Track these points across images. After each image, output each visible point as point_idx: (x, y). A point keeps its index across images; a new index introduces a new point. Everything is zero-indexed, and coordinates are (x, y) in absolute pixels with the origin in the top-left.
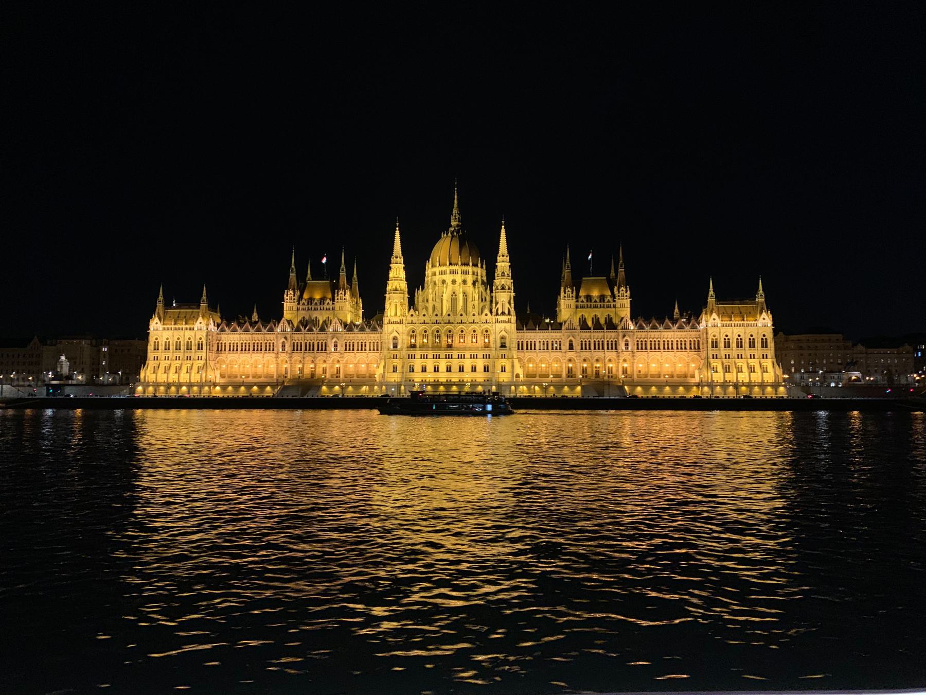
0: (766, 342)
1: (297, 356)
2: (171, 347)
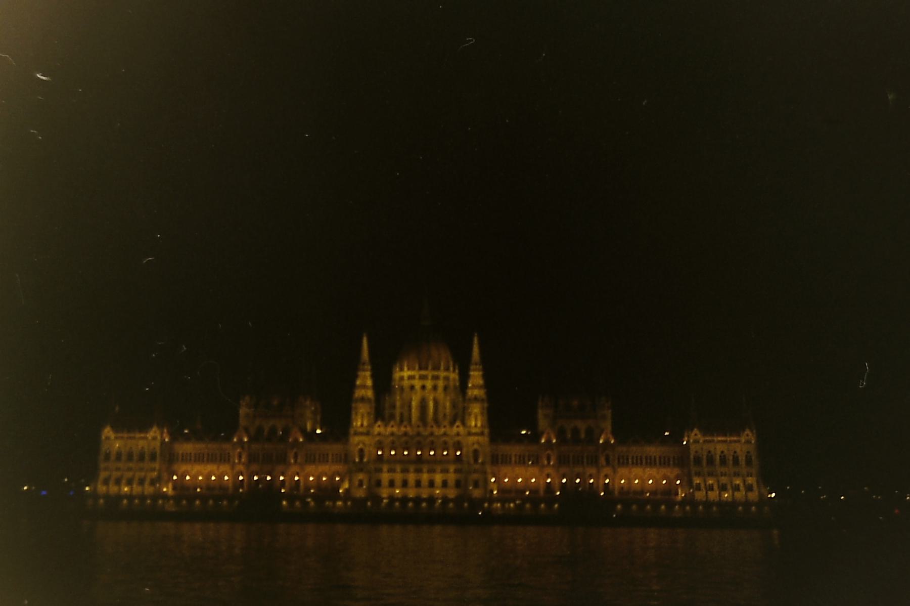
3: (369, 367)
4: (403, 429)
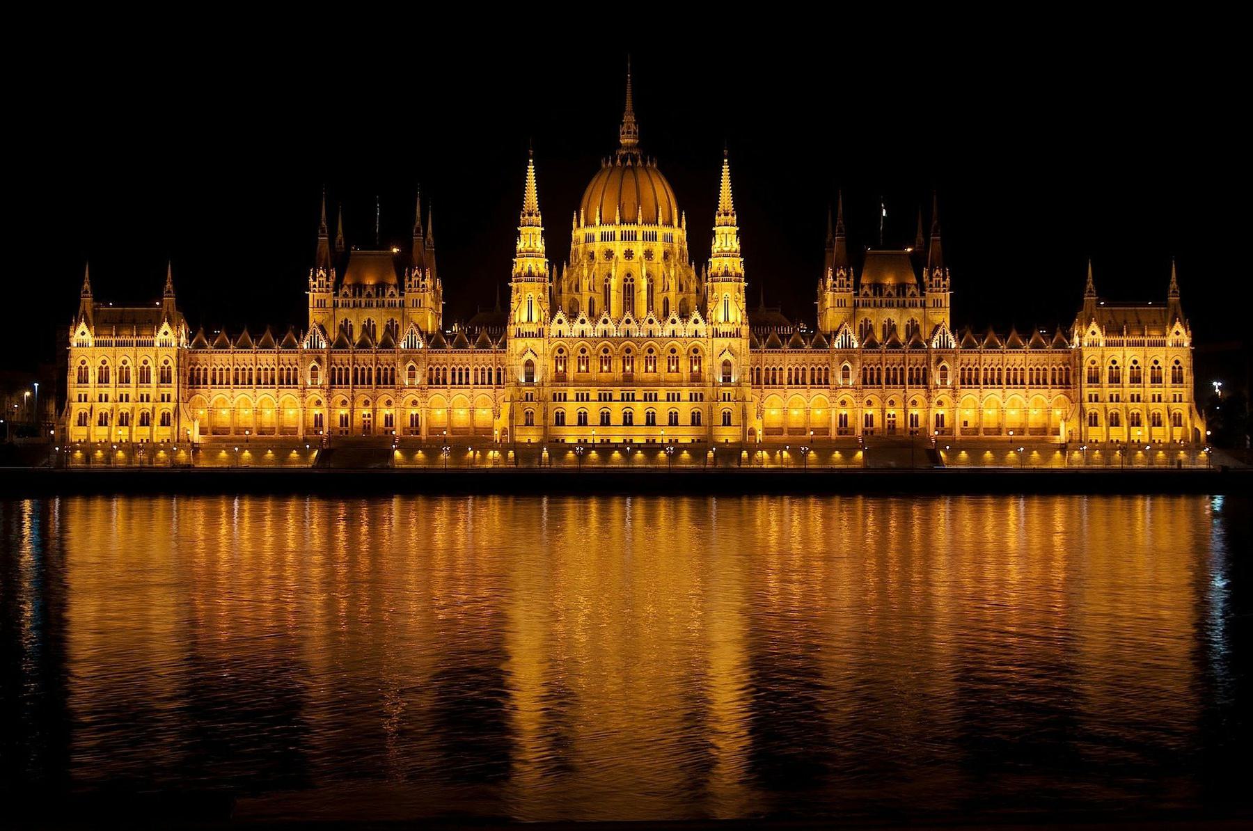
0: (1181, 373)
1: (340, 394)
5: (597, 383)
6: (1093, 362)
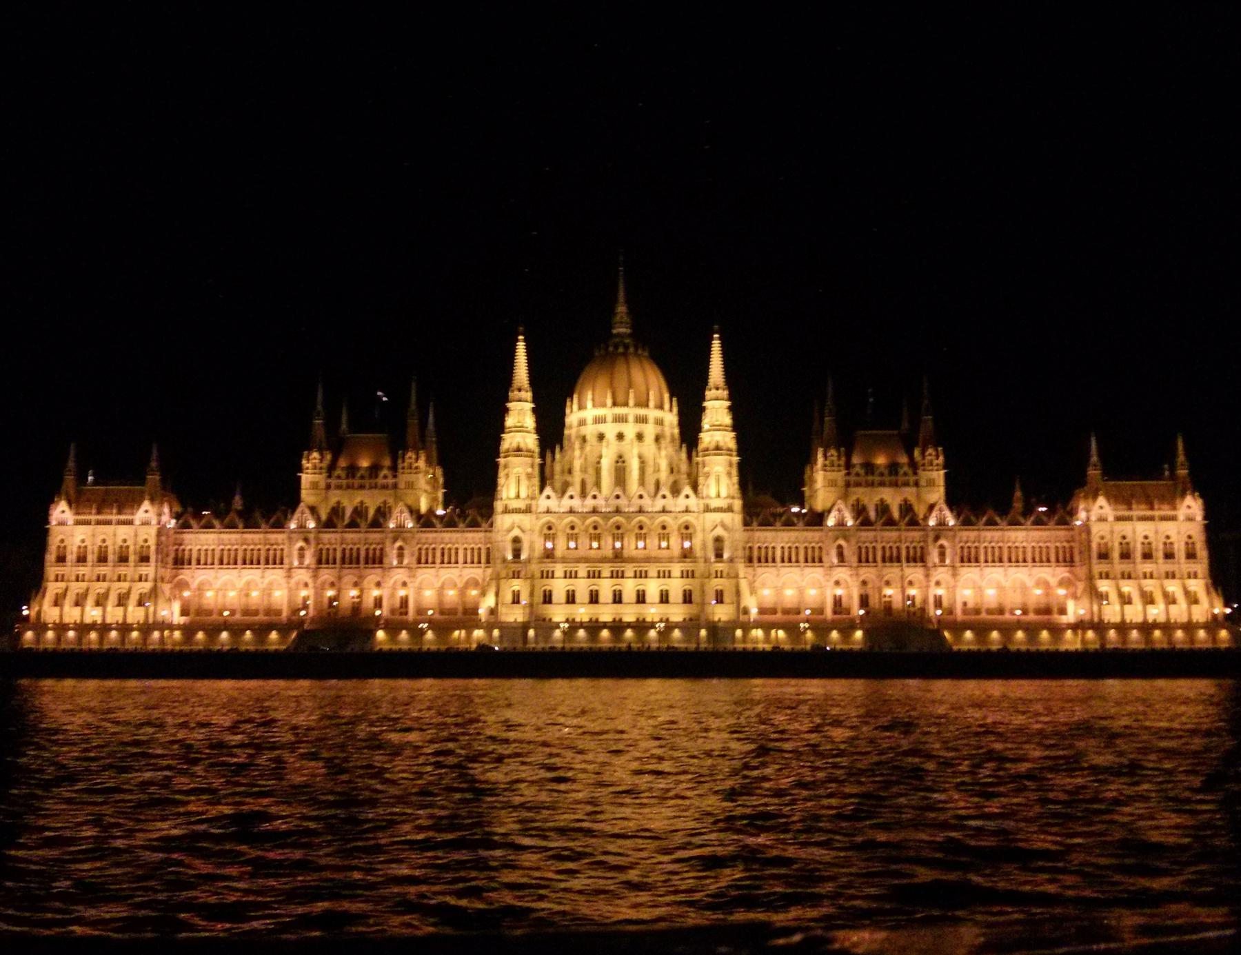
1: (327, 574)
2: (90, 558)
3: (529, 395)
4: (590, 502)
5: (586, 560)
6: (1102, 538)
